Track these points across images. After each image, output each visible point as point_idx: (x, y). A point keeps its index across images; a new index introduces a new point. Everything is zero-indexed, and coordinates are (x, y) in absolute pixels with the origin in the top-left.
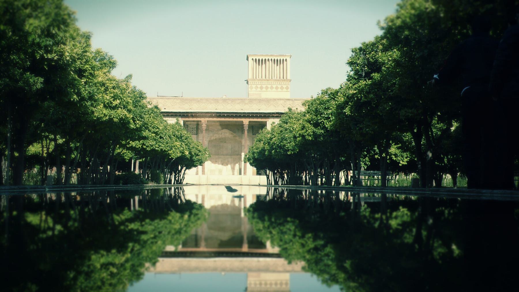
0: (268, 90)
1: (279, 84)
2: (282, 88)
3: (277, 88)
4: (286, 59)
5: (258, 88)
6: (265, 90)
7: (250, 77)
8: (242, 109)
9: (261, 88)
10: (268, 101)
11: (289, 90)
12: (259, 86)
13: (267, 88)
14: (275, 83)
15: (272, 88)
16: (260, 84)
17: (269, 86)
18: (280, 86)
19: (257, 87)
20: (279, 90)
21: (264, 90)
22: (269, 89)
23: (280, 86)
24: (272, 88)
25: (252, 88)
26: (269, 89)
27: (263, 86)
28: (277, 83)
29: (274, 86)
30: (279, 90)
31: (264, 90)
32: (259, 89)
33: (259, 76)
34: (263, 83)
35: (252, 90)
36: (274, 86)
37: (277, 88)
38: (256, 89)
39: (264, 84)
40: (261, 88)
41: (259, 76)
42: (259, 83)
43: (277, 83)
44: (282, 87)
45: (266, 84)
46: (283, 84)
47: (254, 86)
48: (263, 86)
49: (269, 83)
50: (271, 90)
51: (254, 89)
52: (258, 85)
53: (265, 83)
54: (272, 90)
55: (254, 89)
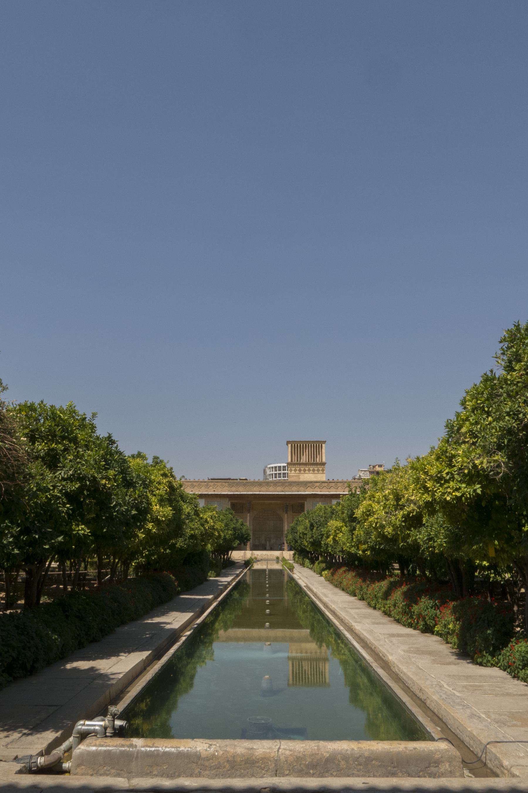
0: (306, 472)
3: (314, 470)
5: (297, 470)
6: (303, 472)
8: (283, 491)
9: (300, 470)
10: (306, 484)
11: (324, 472)
12: (298, 469)
13: (305, 470)
15: (309, 470)
17: (307, 469)
18: (316, 469)
20: (316, 472)
21: (302, 472)
22: (307, 472)
23: (316, 469)
24: (309, 470)
25: (291, 471)
26: (307, 472)
27: (301, 468)
29: (311, 469)
30: (316, 472)
31: (302, 472)
32: (297, 472)
36: (311, 469)
37: (314, 470)
40: (300, 470)
44: (318, 469)
47: (293, 469)
51: (293, 472)
55: (293, 472)
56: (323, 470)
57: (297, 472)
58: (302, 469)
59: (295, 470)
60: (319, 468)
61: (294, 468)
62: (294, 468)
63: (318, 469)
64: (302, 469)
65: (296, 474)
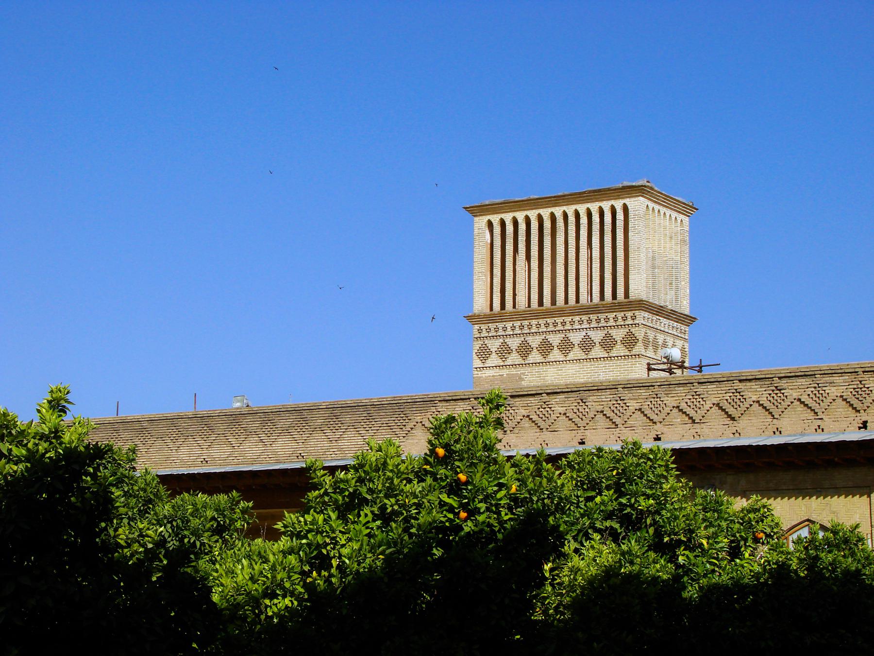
1: (594, 324)
2: (608, 343)
3: (587, 345)
4: (625, 208)
7: (480, 304)
9: (525, 350)
12: (514, 343)
13: (546, 348)
14: (581, 322)
15: (566, 346)
16: (518, 331)
18: (597, 336)
19: (504, 351)
22: (556, 355)
24: (566, 346)
25: (484, 353)
26: (556, 355)
28: (589, 321)
29: (576, 338)
33: (515, 295)
34: (530, 326)
35: (489, 363)
37: (587, 345)
38: (503, 358)
40: (525, 350)
41: (515, 295)
42: (513, 328)
43: (589, 321)
44: (608, 336)
45: (543, 329)
46: (612, 323)
48: (530, 339)
49: (555, 324)
51: (494, 360)
52: (509, 341)
53: (538, 326)
54: (571, 356)
55: (494, 360)
56: (630, 341)
57: (509, 362)
58: (535, 341)
59: (504, 351)
63: (608, 336)
64: (535, 341)
65: (505, 372)
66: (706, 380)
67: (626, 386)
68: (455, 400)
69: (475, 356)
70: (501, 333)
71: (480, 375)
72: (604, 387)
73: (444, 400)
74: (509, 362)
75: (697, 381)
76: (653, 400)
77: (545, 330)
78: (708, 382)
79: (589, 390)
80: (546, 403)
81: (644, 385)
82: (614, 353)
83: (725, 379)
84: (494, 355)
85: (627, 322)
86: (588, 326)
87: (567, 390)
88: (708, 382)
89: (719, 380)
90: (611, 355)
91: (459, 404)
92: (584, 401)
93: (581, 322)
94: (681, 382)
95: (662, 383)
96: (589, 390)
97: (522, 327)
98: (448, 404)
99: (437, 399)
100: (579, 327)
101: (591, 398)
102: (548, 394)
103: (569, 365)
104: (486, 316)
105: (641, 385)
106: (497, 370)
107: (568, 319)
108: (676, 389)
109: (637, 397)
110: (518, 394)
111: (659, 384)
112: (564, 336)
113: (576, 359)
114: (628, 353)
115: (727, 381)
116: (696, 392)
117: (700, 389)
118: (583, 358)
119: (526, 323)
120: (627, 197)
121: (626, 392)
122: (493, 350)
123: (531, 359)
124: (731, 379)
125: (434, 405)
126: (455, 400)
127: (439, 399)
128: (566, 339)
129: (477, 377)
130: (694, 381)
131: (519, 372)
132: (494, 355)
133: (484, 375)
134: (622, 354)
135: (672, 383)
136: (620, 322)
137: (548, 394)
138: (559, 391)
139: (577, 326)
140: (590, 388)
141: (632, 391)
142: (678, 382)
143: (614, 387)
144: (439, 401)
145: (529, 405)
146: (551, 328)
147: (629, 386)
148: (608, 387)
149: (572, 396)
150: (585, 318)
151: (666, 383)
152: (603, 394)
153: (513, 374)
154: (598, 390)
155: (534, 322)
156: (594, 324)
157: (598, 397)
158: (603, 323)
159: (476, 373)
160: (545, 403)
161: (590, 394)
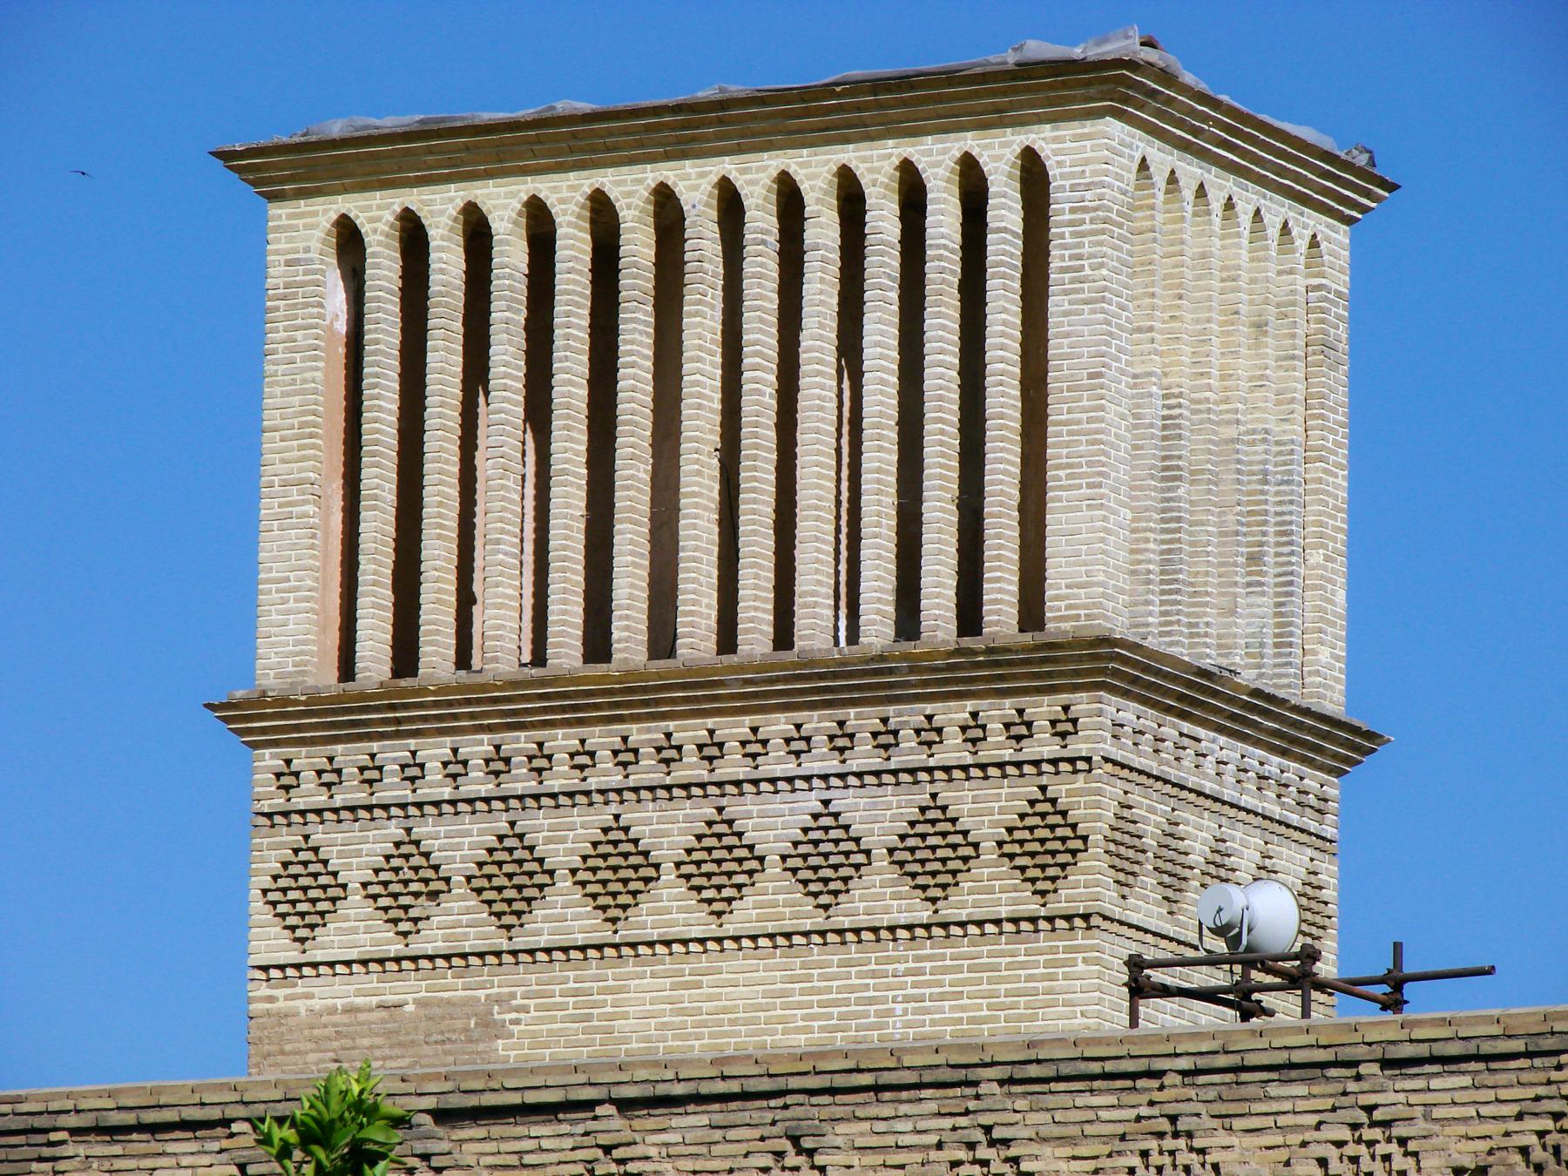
1: (864, 757)
4: (1033, 174)
14: (799, 743)
16: (477, 784)
28: (843, 740)
33: (466, 600)
34: (540, 762)
35: (331, 942)
38: (402, 919)
39: (561, 778)
41: (466, 600)
42: (456, 768)
43: (843, 740)
44: (935, 815)
45: (606, 774)
48: (539, 825)
49: (668, 754)
50: (697, 922)
52: (432, 832)
53: (584, 759)
54: (746, 915)
60: (963, 799)
61: (378, 839)
62: (378, 839)
63: (935, 815)
65: (409, 990)
66: (1422, 1050)
67: (1020, 1073)
68: (154, 1129)
69: (257, 904)
70: (393, 789)
71: (281, 1004)
72: (911, 1078)
73: (99, 1130)
74: (431, 940)
75: (1377, 1052)
76: (1152, 1144)
77: (616, 779)
78: (1433, 1060)
79: (832, 1091)
80: (616, 1153)
81: (1109, 1067)
82: (963, 903)
83: (1518, 1045)
84: (355, 906)
85: (1031, 750)
86: (833, 765)
87: (721, 1087)
88: (1433, 1060)
89: (1487, 1048)
90: (947, 912)
91: (171, 1148)
92: (807, 1143)
93: (799, 743)
94: (1298, 1057)
95: (1202, 1062)
96: (832, 1091)
97: (499, 764)
98: (117, 1149)
99: (64, 1121)
100: (790, 767)
101: (841, 1128)
102: (625, 1106)
103: (734, 964)
104: (317, 705)
105: (1095, 1068)
106: (372, 981)
107: (734, 729)
108: (1273, 1090)
109: (1074, 1131)
110: (472, 1101)
111: (1184, 1063)
112: (710, 812)
113: (771, 927)
114: (1033, 907)
115: (1529, 1055)
116: (1369, 1109)
117: (1392, 1095)
118: (808, 925)
119: (520, 743)
120: (1040, 120)
121: (1021, 1104)
122: (354, 876)
123: (542, 927)
124: (1549, 1043)
125: (47, 1152)
126: (154, 1129)
127: (73, 1121)
128: (723, 829)
129: (268, 1014)
130: (1360, 1052)
131: (482, 994)
132: (355, 906)
133: (301, 1006)
134: (1004, 912)
135: (1252, 1059)
136: (997, 747)
137: (625, 1106)
138: (679, 1089)
139: (777, 763)
140: (840, 1081)
141: (1051, 1101)
142: (1280, 1058)
143: (960, 1075)
144: (74, 1131)
145: (528, 1159)
146: (648, 771)
147: (1033, 1071)
148: (928, 1077)
149: (744, 1117)
150: (818, 722)
151: (1222, 1061)
152: (904, 1109)
153: (449, 1002)
154: (877, 1089)
155: (562, 740)
156: (864, 757)
157: (881, 1126)
158: (909, 753)
159: (264, 990)
160: (607, 1149)
161: (839, 1112)
